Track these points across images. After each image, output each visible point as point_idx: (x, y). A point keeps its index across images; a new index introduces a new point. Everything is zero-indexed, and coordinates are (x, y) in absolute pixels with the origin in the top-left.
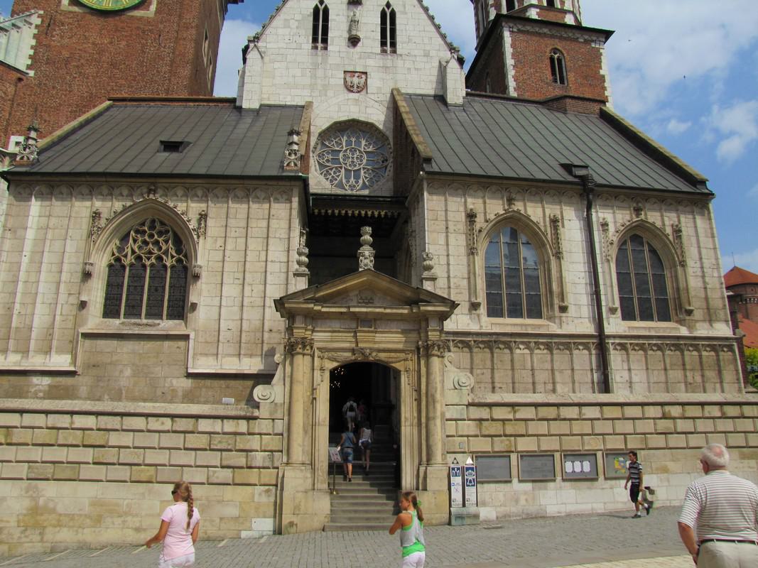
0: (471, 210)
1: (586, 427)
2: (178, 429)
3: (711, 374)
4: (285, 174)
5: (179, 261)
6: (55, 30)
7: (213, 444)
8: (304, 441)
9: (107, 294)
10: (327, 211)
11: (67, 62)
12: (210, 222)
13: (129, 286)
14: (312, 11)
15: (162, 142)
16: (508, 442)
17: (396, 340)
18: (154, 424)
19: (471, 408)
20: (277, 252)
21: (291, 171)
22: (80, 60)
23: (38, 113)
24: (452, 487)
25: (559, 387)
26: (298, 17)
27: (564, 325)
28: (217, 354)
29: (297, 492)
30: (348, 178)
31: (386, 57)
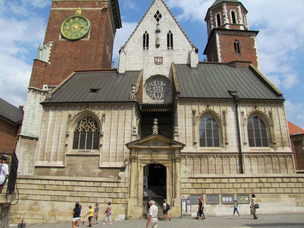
0: (194, 110)
1: (231, 186)
2: (95, 186)
3: (283, 166)
4: (130, 100)
5: (97, 130)
6: (57, 48)
7: (107, 191)
8: (134, 190)
9: (74, 141)
10: (146, 110)
11: (61, 58)
12: (106, 117)
13: (81, 139)
15: (91, 89)
16: (202, 191)
17: (165, 156)
18: (88, 184)
19: (190, 179)
20: (128, 127)
21: (132, 99)
22: (65, 57)
23: (52, 77)
24: (182, 206)
25: (225, 171)
26: (138, 38)
27: (227, 149)
28: (109, 161)
29: (132, 206)
30: (156, 95)
31: (169, 51)
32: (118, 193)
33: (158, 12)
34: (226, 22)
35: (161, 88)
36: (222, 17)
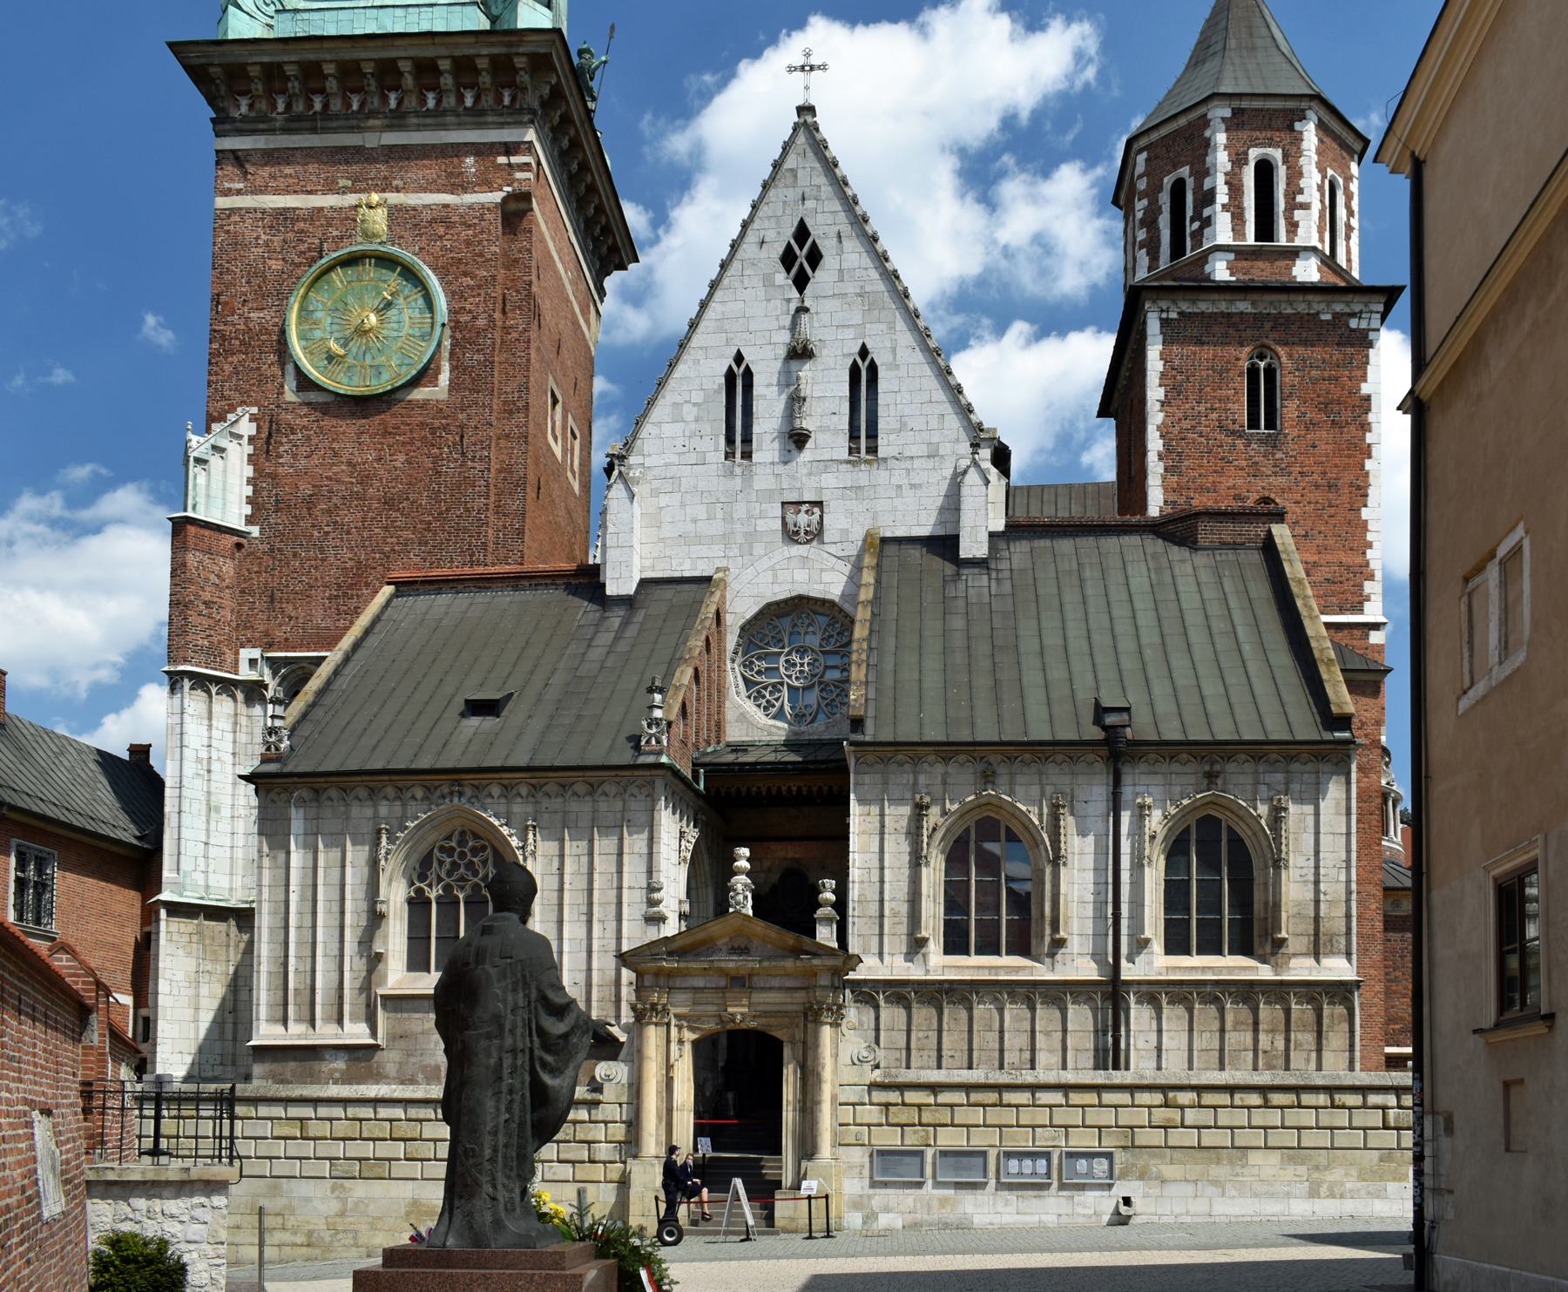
1: (1042, 1116)
14: (723, 380)
26: (697, 397)
27: (1058, 967)
32: (594, 1142)
34: (1214, 236)
36: (1195, 200)
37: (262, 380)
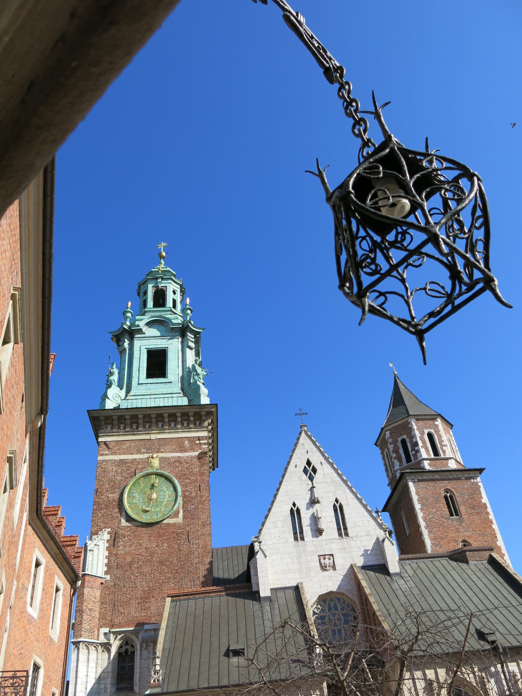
6: (120, 542)
11: (130, 564)
22: (138, 562)
26: (282, 519)
31: (343, 541)
33: (309, 463)
34: (421, 456)
35: (339, 620)
36: (411, 445)
37: (113, 518)
